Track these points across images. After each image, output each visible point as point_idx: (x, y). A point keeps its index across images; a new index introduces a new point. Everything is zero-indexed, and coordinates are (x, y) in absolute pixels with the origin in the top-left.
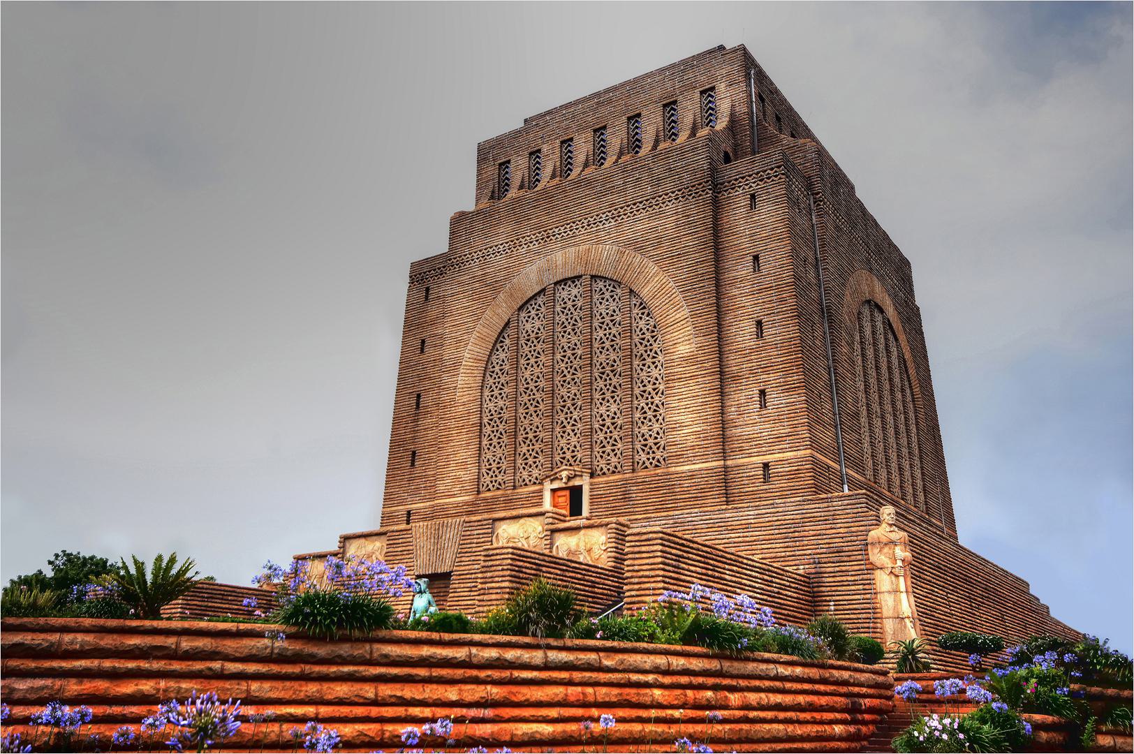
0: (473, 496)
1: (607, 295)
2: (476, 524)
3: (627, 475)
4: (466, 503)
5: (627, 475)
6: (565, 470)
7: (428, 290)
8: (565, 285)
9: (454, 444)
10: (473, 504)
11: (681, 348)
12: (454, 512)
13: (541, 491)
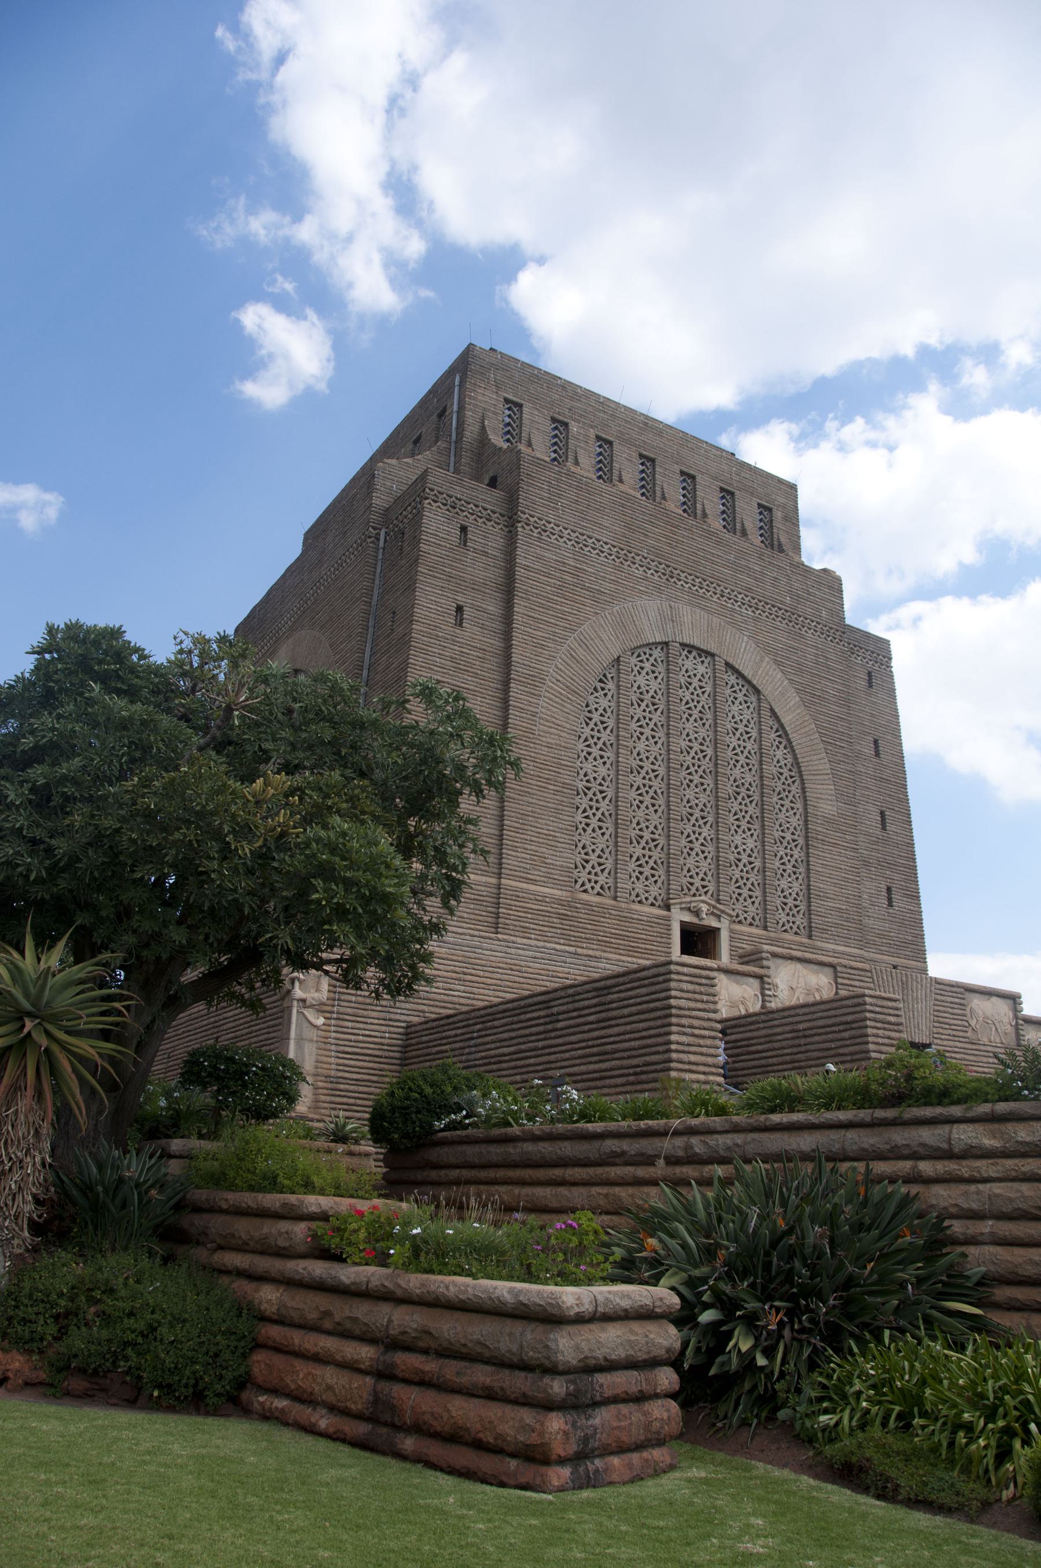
0: (568, 894)
1: (740, 697)
2: (948, 988)
3: (772, 935)
4: (559, 901)
5: (772, 935)
6: (703, 902)
7: (464, 529)
8: (690, 652)
9: (534, 801)
10: (569, 905)
11: (825, 806)
12: (536, 907)
13: (668, 919)
